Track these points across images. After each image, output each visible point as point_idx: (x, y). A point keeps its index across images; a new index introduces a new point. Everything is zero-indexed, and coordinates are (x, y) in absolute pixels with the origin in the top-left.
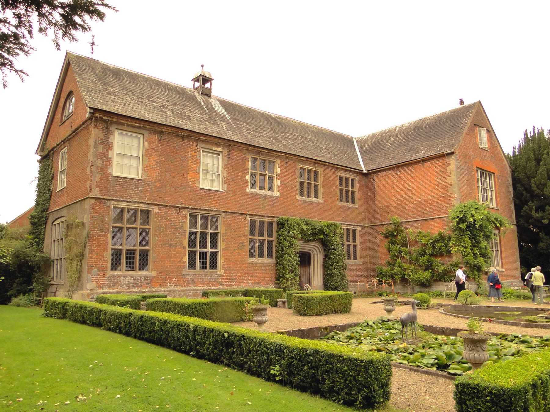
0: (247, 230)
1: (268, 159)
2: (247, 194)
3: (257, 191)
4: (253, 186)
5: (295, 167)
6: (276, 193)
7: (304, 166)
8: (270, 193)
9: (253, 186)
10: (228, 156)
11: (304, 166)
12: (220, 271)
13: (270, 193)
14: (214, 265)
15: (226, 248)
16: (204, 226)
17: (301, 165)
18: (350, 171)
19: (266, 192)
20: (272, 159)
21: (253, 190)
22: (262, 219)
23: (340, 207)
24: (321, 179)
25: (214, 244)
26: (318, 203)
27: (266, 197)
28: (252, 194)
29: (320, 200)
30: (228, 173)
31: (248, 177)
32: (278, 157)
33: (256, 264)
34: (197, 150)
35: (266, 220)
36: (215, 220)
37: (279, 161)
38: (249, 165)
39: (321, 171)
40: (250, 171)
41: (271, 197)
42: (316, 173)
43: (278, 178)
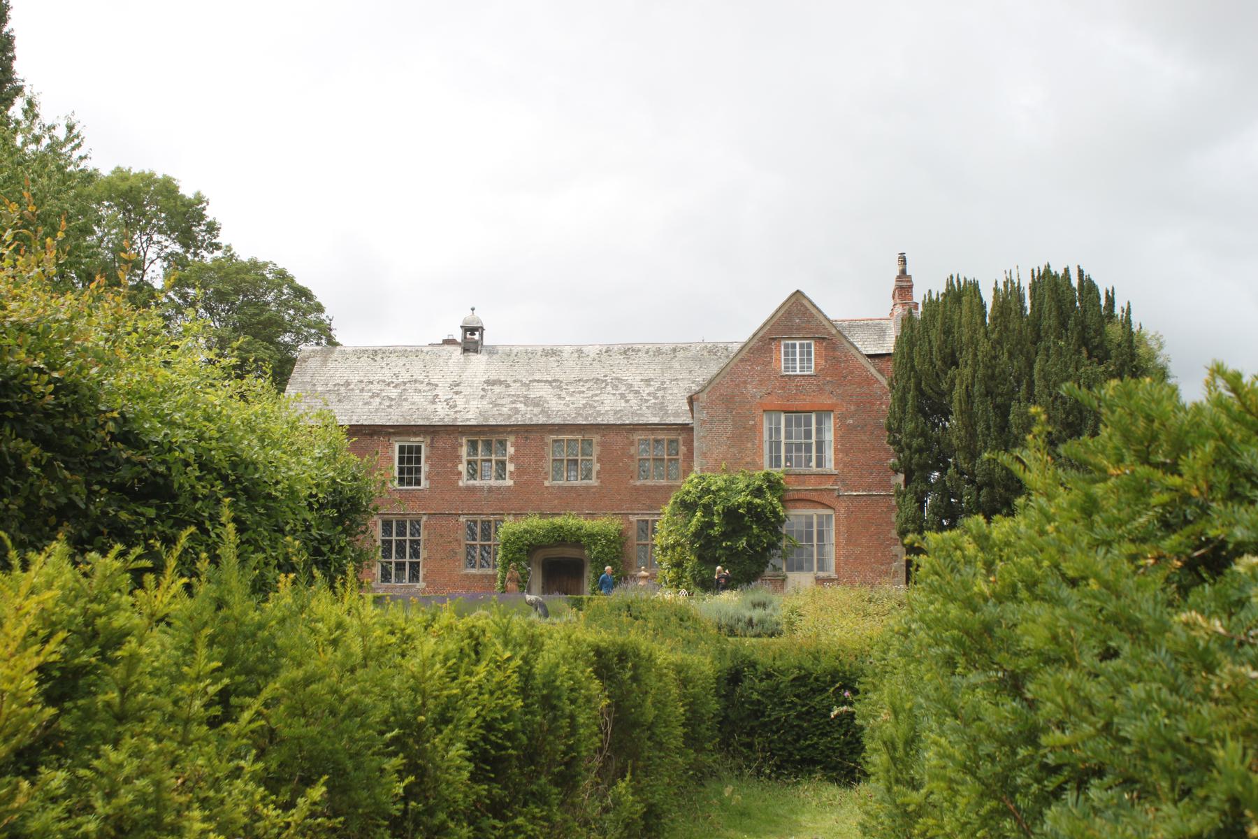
0: (462, 534)
1: (494, 438)
2: (460, 489)
3: (478, 483)
4: (472, 476)
5: (542, 439)
6: (509, 482)
7: (561, 437)
8: (500, 483)
9: (472, 476)
10: (431, 445)
11: (561, 437)
12: (421, 585)
13: (500, 483)
14: (414, 577)
15: (429, 557)
16: (401, 532)
17: (555, 437)
18: (662, 429)
19: (493, 483)
20: (501, 437)
21: (472, 482)
22: (484, 518)
23: (636, 488)
24: (596, 450)
25: (415, 553)
26: (587, 488)
27: (490, 489)
28: (468, 488)
29: (594, 482)
30: (432, 467)
31: (462, 468)
32: (511, 432)
33: (474, 576)
34: (390, 446)
35: (491, 518)
36: (416, 523)
37: (511, 440)
38: (464, 451)
39: (596, 438)
40: (465, 457)
41: (499, 488)
42: (590, 443)
43: (511, 460)
